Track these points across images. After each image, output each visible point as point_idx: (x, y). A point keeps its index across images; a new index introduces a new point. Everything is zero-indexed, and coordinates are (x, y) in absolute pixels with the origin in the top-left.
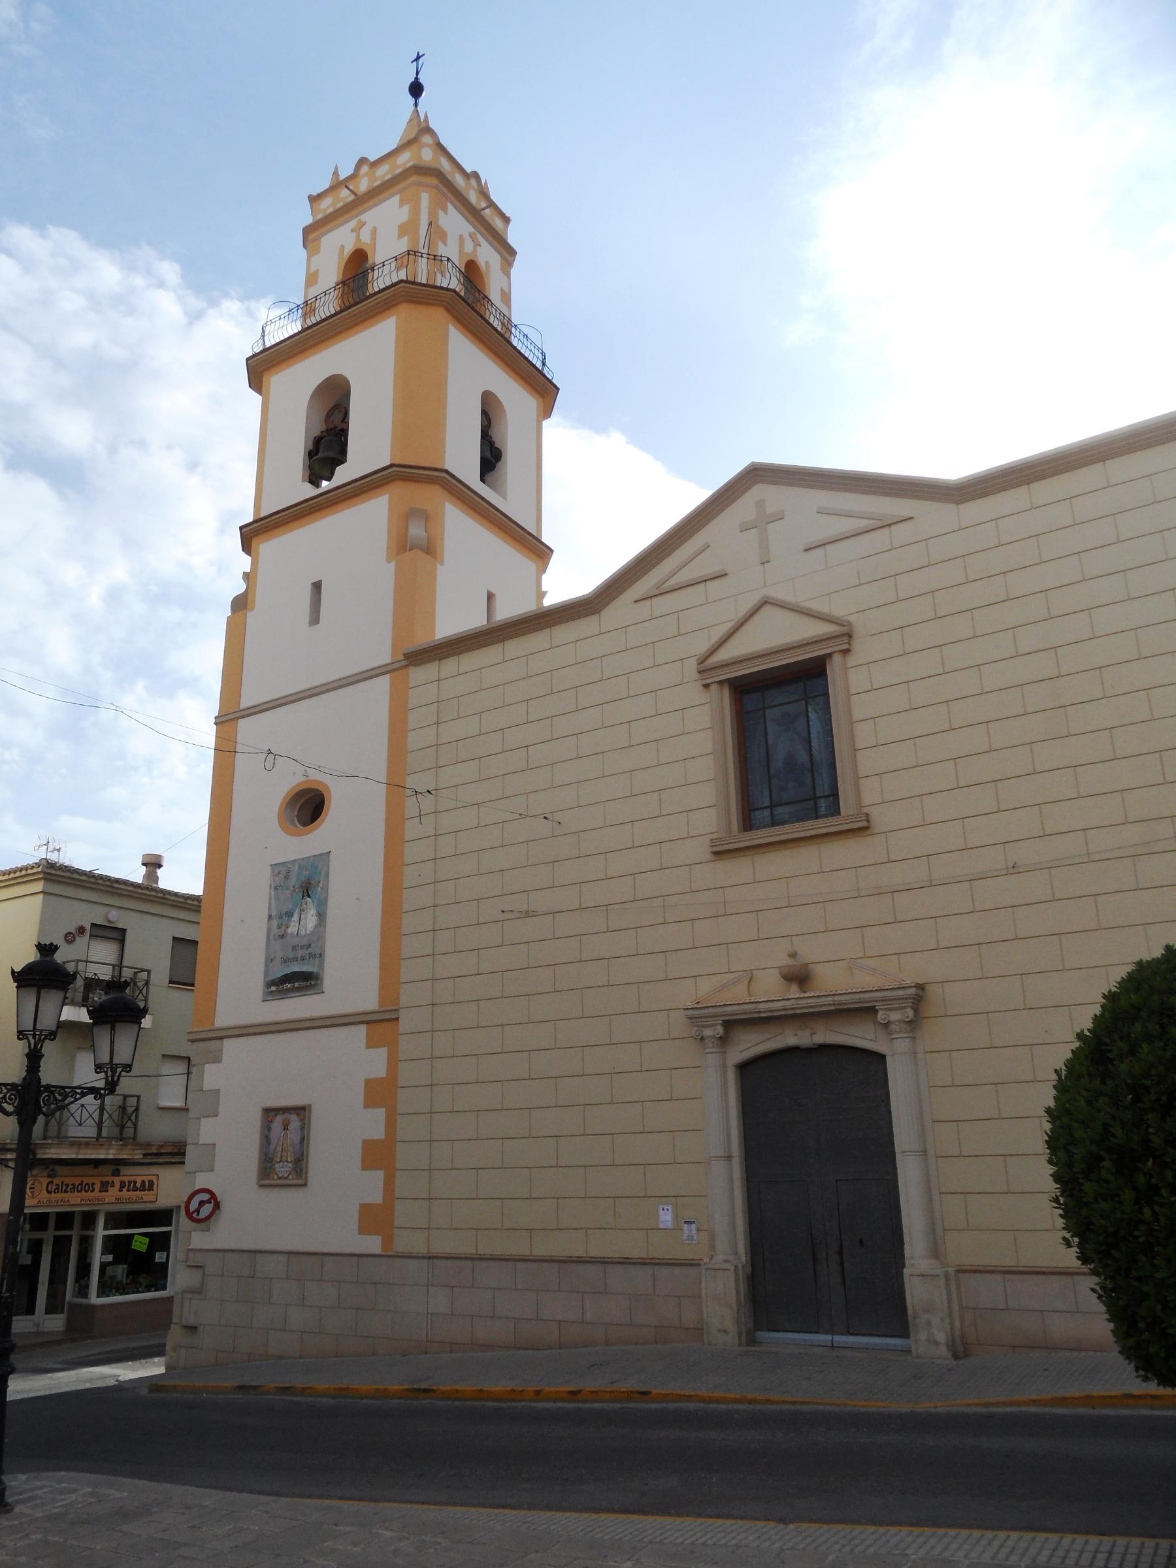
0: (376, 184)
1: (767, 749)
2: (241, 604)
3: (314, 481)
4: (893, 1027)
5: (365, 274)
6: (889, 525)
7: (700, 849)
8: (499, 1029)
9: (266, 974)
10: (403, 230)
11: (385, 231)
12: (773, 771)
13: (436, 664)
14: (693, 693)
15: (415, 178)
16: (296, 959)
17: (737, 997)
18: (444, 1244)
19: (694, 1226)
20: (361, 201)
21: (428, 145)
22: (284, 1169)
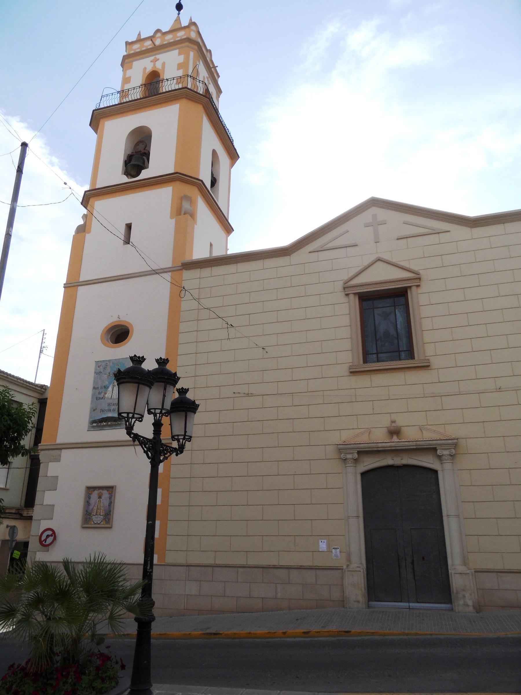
0: (165, 43)
1: (375, 326)
2: (82, 230)
3: (127, 173)
4: (444, 457)
5: (158, 82)
6: (439, 233)
7: (344, 370)
8: (231, 451)
9: (90, 417)
10: (180, 66)
11: (171, 66)
12: (377, 337)
13: (209, 269)
14: (341, 297)
15: (187, 44)
16: (109, 410)
17: (364, 440)
18: (194, 559)
19: (338, 550)
20: (156, 49)
21: (194, 31)
22: (97, 519)
